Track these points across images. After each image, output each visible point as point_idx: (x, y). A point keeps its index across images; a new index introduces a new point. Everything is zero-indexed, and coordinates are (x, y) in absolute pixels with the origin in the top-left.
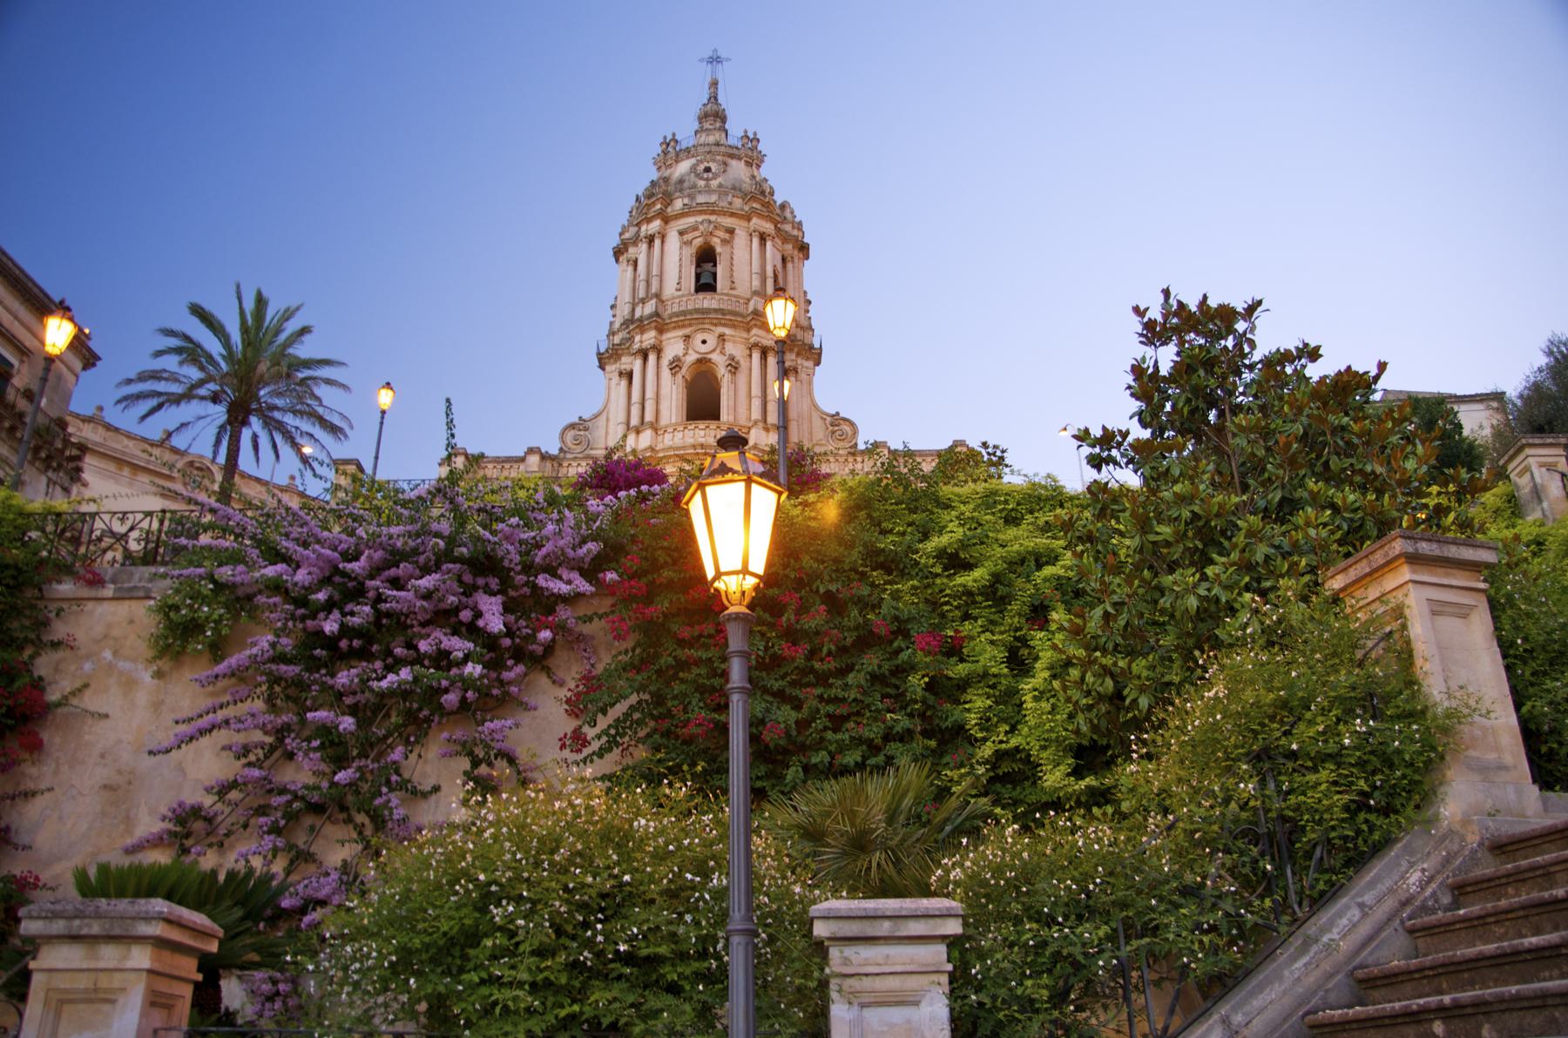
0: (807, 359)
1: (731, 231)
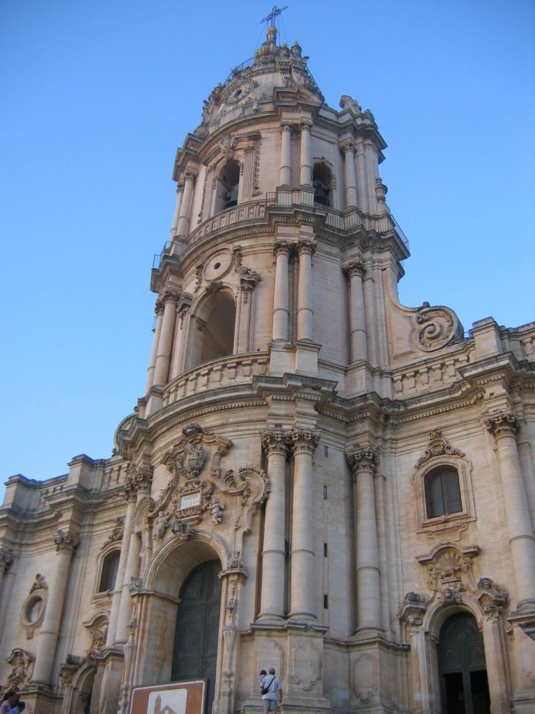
0: (381, 251)
1: (256, 137)
